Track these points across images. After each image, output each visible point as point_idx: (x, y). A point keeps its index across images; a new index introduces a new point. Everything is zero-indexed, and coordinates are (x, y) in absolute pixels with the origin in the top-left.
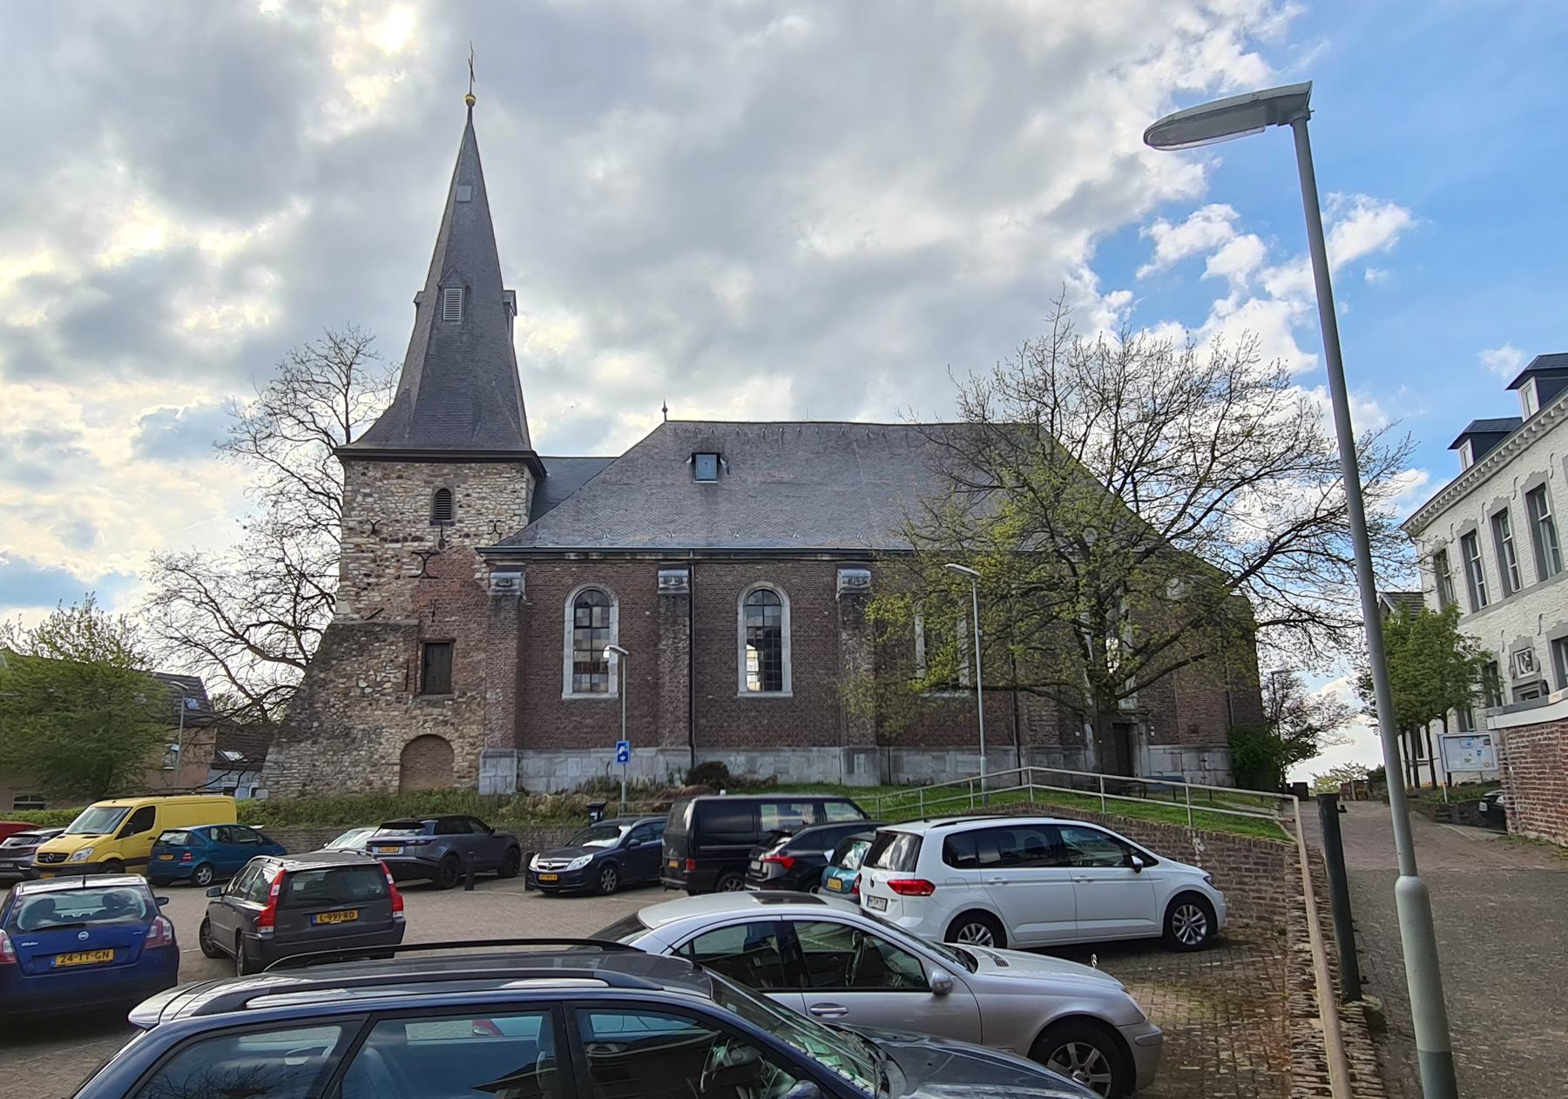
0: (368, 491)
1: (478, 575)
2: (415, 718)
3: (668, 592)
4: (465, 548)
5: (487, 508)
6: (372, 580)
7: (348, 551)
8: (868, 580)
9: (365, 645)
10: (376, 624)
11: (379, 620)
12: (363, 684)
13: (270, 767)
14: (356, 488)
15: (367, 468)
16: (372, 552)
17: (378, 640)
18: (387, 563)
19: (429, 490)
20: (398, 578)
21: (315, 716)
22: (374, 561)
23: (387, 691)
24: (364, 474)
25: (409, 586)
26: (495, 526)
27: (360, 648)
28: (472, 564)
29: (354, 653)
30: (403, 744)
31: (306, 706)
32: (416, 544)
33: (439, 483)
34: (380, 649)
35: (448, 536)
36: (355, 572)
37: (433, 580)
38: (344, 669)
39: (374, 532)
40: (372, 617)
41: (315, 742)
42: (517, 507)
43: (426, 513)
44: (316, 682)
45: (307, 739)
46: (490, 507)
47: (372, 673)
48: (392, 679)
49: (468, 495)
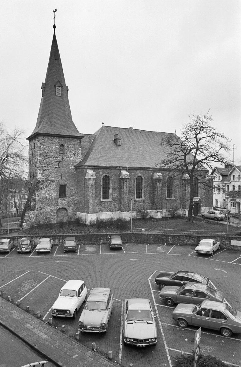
5: (72, 150)
6: (46, 168)
19: (59, 145)
24: (43, 139)
26: (74, 155)
28: (70, 165)
29: (44, 187)
32: (56, 159)
33: (61, 143)
39: (46, 156)
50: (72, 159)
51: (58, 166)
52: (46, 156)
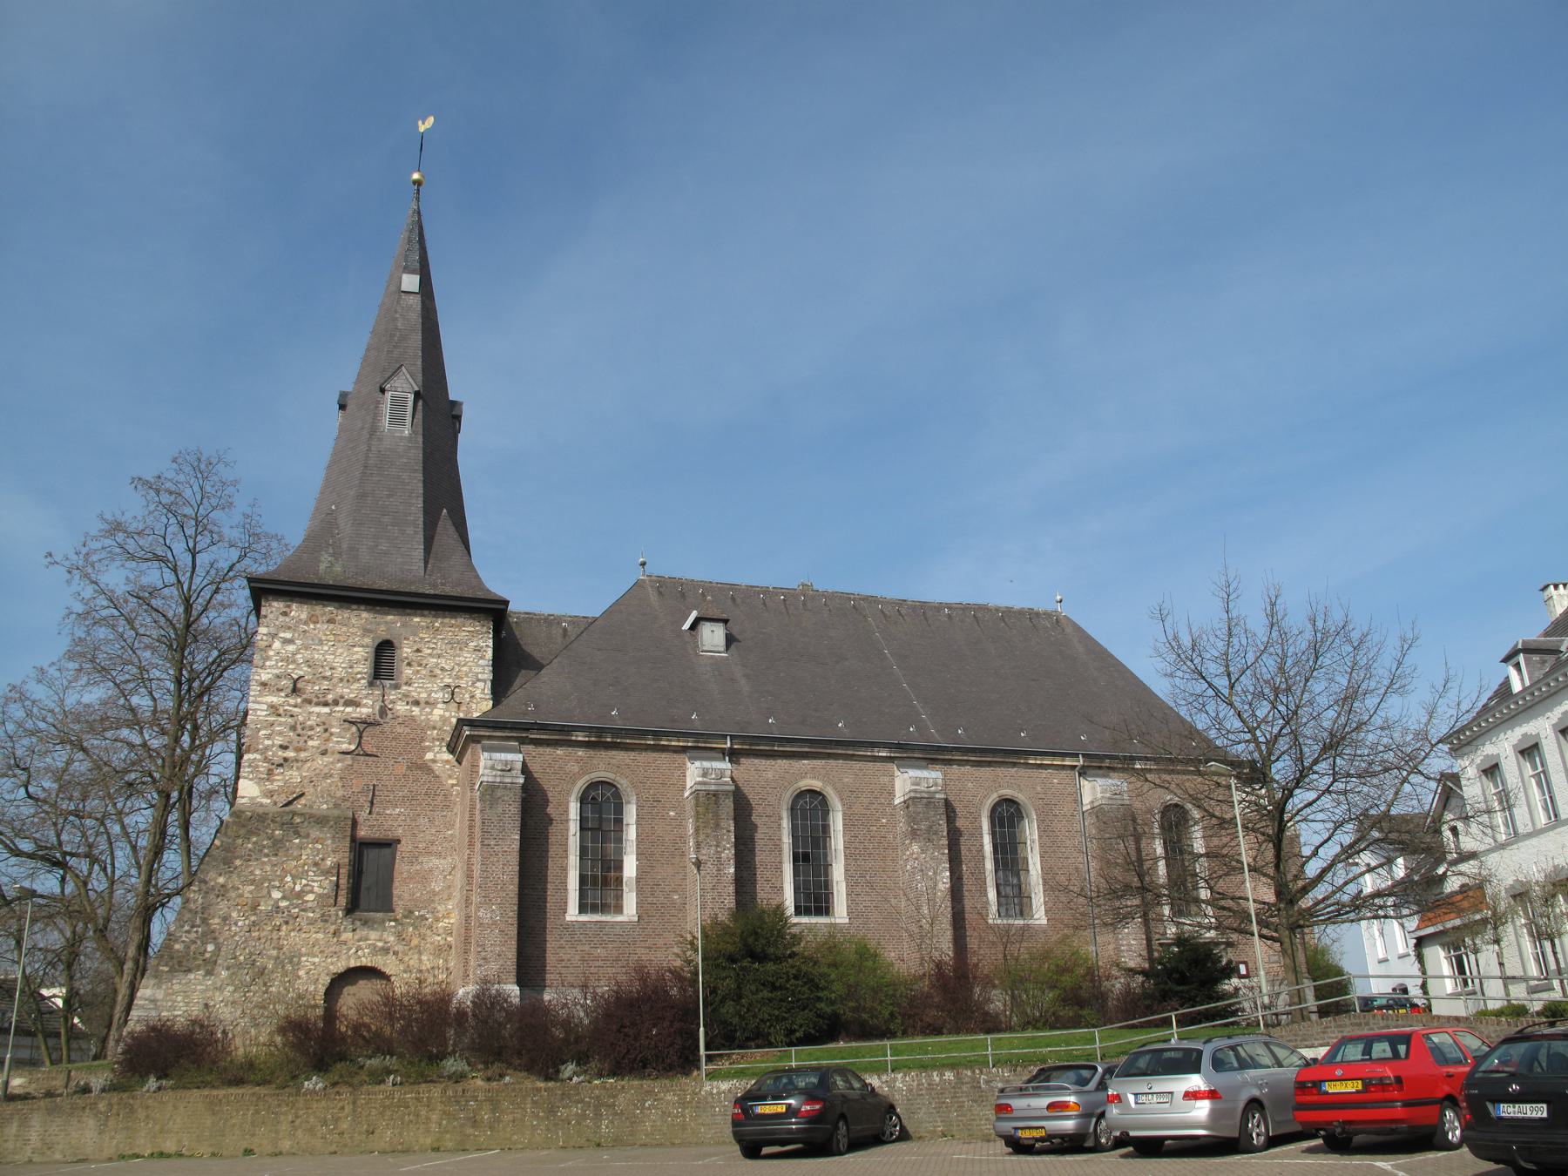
0: (288, 635)
1: (429, 756)
2: (345, 943)
3: (707, 788)
4: (413, 719)
5: (443, 669)
6: (290, 754)
7: (259, 713)
8: (940, 781)
9: (281, 841)
10: (294, 814)
11: (298, 806)
13: (142, 1007)
14: (273, 630)
15: (289, 606)
16: (292, 716)
17: (298, 834)
18: (310, 733)
19: (367, 640)
20: (324, 753)
21: (210, 936)
22: (293, 728)
23: (309, 905)
24: (285, 614)
25: (339, 765)
26: (453, 694)
27: (274, 845)
28: (423, 740)
29: (266, 851)
30: (328, 980)
31: (198, 922)
32: (349, 709)
33: (383, 634)
35: (393, 702)
36: (267, 742)
37: (371, 759)
38: (252, 873)
39: (295, 690)
41: (209, 973)
42: (480, 670)
43: (365, 668)
44: (213, 888)
45: (198, 968)
46: (447, 667)
47: (289, 879)
48: (316, 889)
49: (418, 651)
50: (438, 712)
51: (360, 744)
52: (295, 690)
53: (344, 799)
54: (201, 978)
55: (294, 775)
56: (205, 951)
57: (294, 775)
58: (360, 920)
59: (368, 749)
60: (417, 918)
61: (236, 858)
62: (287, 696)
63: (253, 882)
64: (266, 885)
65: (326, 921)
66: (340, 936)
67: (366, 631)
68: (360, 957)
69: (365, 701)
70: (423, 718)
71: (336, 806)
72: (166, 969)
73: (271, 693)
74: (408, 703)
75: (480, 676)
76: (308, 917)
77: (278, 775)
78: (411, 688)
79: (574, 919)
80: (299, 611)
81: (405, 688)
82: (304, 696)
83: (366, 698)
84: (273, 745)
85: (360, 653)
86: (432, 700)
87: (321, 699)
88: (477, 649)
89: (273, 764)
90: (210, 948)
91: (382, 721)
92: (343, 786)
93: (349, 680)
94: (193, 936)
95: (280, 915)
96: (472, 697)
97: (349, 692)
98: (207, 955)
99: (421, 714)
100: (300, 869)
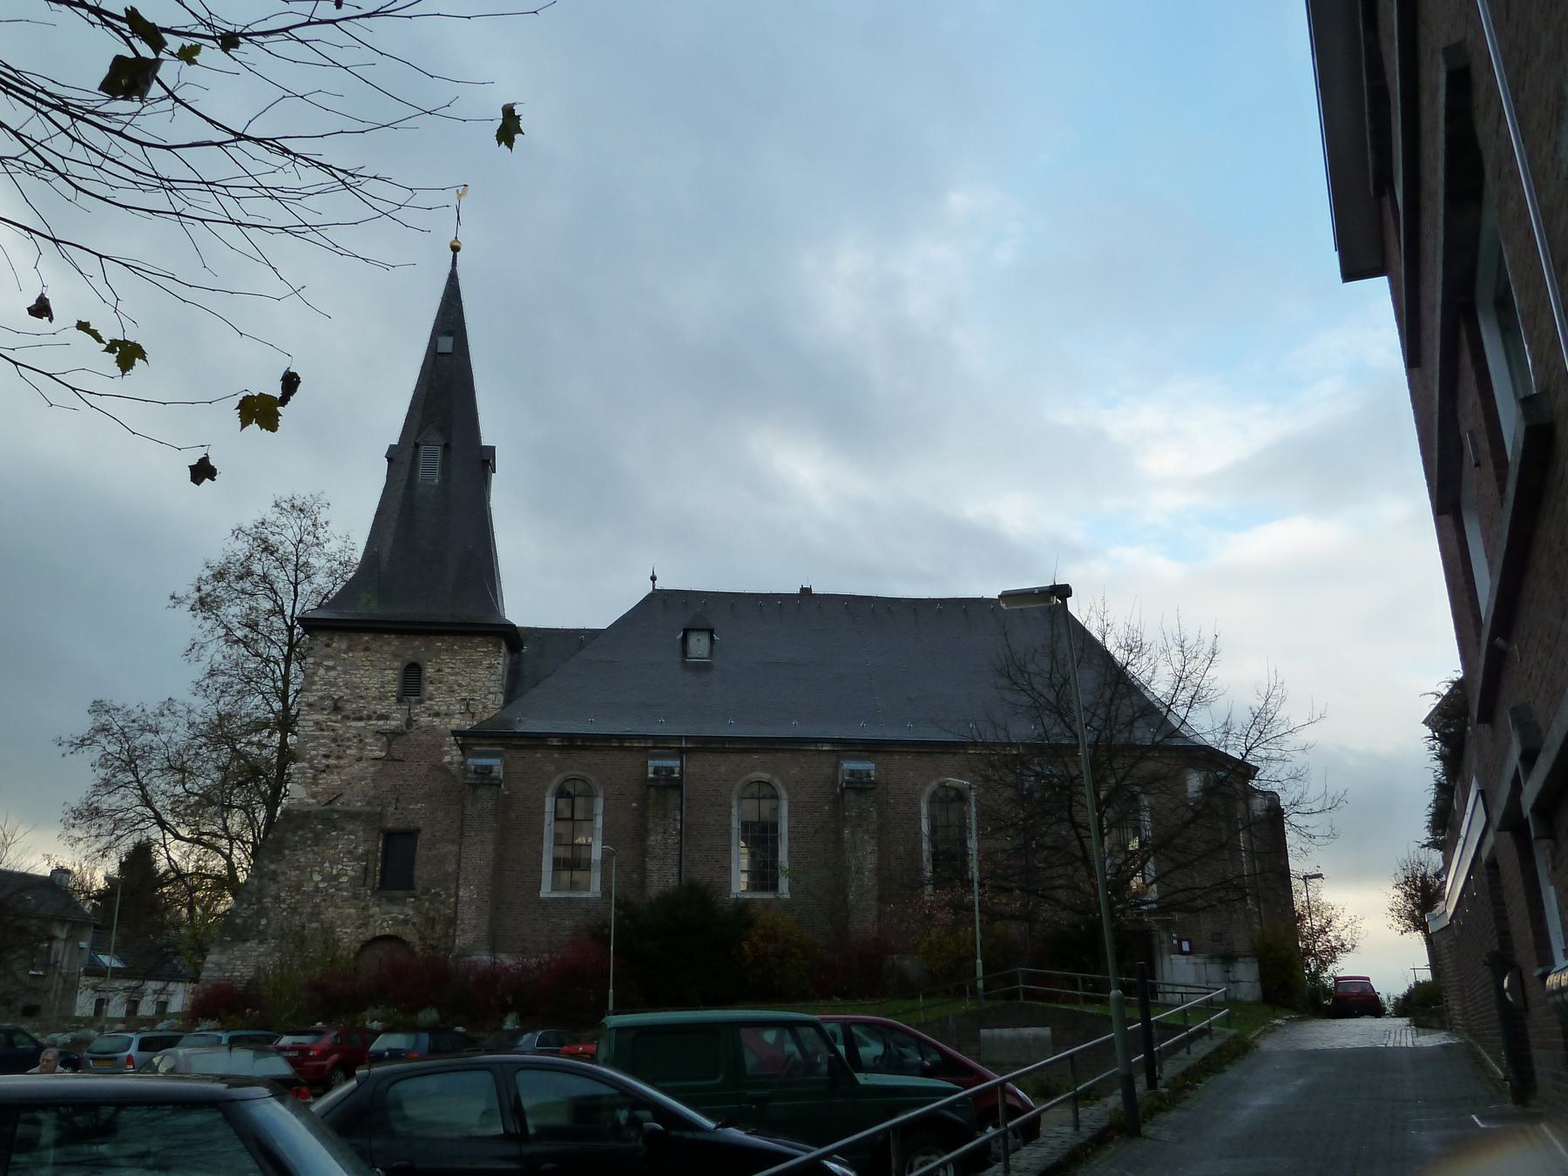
0: (331, 663)
1: (447, 759)
2: (372, 916)
5: (460, 685)
6: (332, 762)
10: (334, 811)
12: (317, 877)
13: (210, 969)
14: (318, 660)
16: (333, 730)
17: (335, 828)
18: (350, 743)
20: (360, 760)
21: (262, 912)
22: (334, 740)
23: (344, 885)
24: (328, 645)
28: (441, 746)
30: (358, 946)
32: (381, 723)
33: (409, 656)
34: (338, 838)
35: (417, 714)
36: (313, 753)
38: (298, 860)
40: (330, 802)
41: (261, 942)
43: (394, 688)
47: (327, 865)
48: (350, 873)
49: (439, 670)
53: (375, 797)
54: (255, 946)
55: (334, 779)
56: (260, 924)
57: (334, 779)
58: (385, 897)
59: (397, 755)
60: (433, 894)
61: (286, 848)
62: (329, 714)
63: (297, 868)
64: (309, 870)
65: (357, 899)
66: (367, 911)
67: (396, 656)
68: (384, 928)
69: (394, 715)
70: (442, 727)
71: (369, 803)
72: (229, 939)
73: (317, 712)
74: (430, 715)
75: (491, 690)
76: (342, 896)
77: (321, 779)
78: (432, 703)
79: (547, 896)
80: (340, 643)
81: (428, 702)
82: (344, 713)
83: (394, 712)
84: (317, 755)
85: (390, 674)
86: (450, 712)
87: (357, 715)
88: (490, 666)
89: (317, 771)
90: (264, 922)
91: (408, 731)
92: (375, 787)
93: (382, 698)
94: (249, 912)
95: (320, 894)
96: (485, 707)
97: (380, 708)
98: (261, 928)
99: (441, 724)
100: (336, 856)
